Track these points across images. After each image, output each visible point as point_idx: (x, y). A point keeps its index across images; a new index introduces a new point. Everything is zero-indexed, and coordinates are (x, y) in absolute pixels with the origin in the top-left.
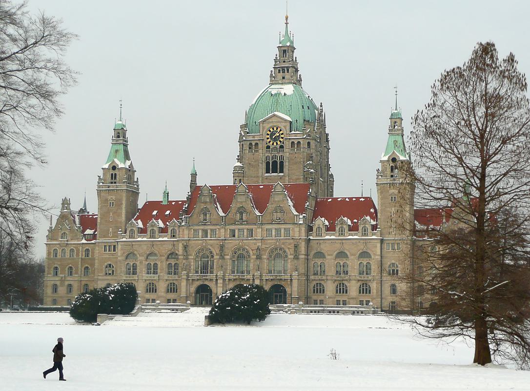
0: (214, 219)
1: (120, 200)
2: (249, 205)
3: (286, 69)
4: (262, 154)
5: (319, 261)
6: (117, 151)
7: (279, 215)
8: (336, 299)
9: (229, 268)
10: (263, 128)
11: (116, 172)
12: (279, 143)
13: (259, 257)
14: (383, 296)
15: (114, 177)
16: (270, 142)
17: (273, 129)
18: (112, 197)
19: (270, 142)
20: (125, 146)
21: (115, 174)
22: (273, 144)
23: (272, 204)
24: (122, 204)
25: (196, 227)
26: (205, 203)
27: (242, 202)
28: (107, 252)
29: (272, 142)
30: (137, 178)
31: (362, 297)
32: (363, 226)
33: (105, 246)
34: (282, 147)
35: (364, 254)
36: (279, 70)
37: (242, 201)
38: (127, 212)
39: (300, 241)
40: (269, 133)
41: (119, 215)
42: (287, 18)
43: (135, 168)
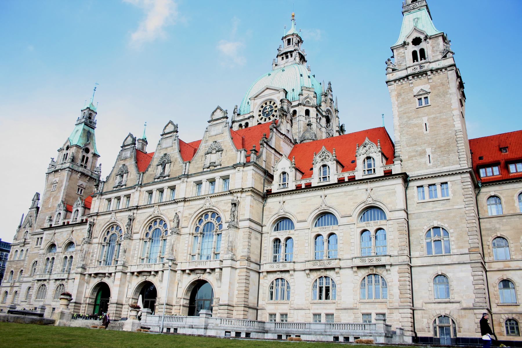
3: (289, 54)
7: (213, 158)
8: (313, 311)
10: (255, 105)
12: (271, 117)
14: (418, 304)
17: (266, 104)
24: (62, 186)
25: (109, 196)
28: (38, 246)
29: (263, 119)
30: (100, 165)
31: (367, 306)
33: (38, 238)
36: (283, 58)
39: (244, 195)
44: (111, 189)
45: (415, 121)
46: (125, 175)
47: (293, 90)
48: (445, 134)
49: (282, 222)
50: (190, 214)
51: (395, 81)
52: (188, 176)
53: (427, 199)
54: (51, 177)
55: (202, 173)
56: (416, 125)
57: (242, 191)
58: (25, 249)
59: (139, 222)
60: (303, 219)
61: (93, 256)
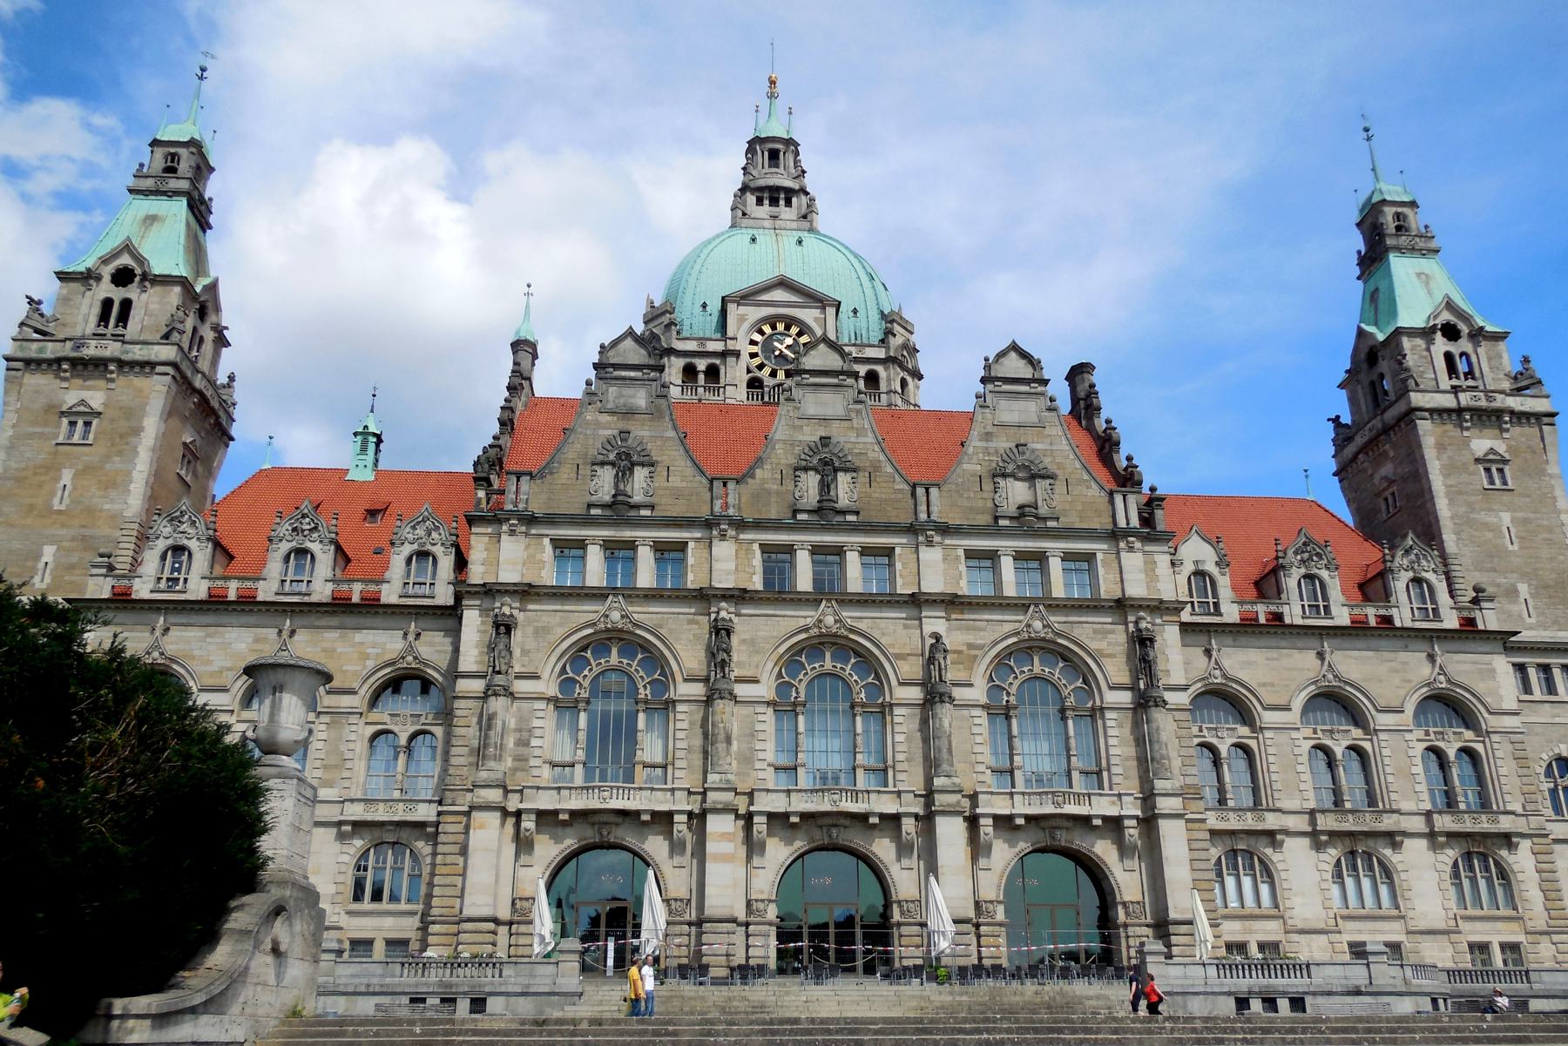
0: (677, 494)
1: (133, 416)
6: (151, 220)
9: (769, 751)
10: (742, 319)
11: (132, 292)
15: (115, 314)
16: (761, 367)
17: (774, 327)
19: (761, 367)
21: (126, 305)
22: (773, 374)
23: (988, 436)
24: (137, 431)
26: (629, 413)
27: (825, 419)
29: (767, 371)
30: (232, 378)
32: (1411, 574)
35: (1449, 705)
37: (829, 412)
40: (757, 337)
41: (116, 483)
42: (772, 83)
45: (1483, 517)
46: (640, 474)
47: (855, 311)
48: (1552, 559)
50: (971, 646)
51: (1432, 411)
52: (945, 530)
53: (1537, 694)
55: (993, 530)
56: (1487, 527)
59: (751, 642)
60: (1282, 702)
61: (523, 743)
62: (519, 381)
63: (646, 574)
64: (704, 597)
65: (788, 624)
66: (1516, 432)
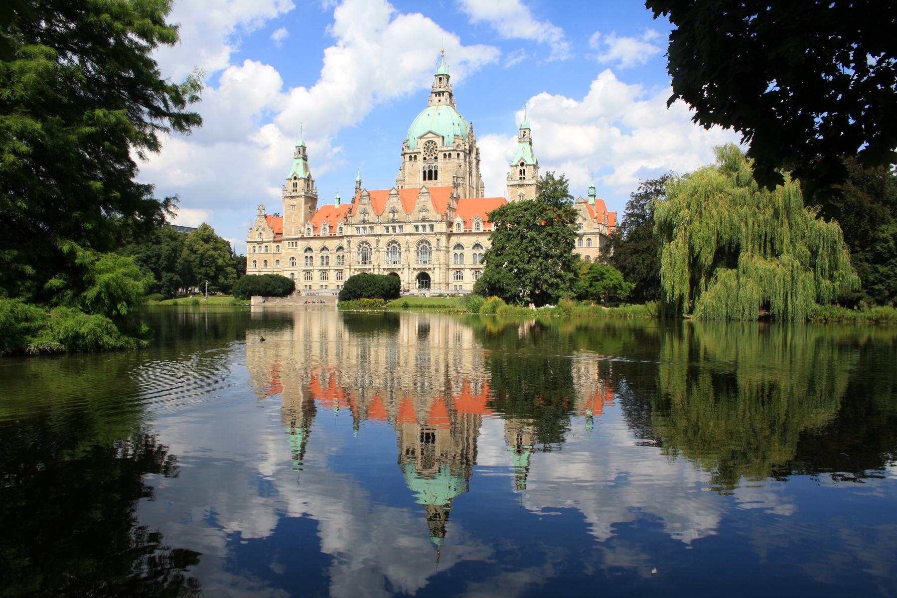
1: (300, 205)
2: (399, 207)
4: (420, 165)
5: (459, 252)
11: (297, 181)
13: (408, 250)
15: (295, 185)
18: (293, 202)
20: (305, 159)
34: (436, 158)
38: (305, 214)
41: (300, 217)
43: (313, 179)
44: (357, 221)
49: (459, 246)
52: (410, 222)
54: (287, 200)
55: (418, 221)
57: (441, 234)
58: (263, 245)
62: (358, 189)
63: (368, 231)
64: (375, 235)
65: (388, 239)
66: (528, 187)
